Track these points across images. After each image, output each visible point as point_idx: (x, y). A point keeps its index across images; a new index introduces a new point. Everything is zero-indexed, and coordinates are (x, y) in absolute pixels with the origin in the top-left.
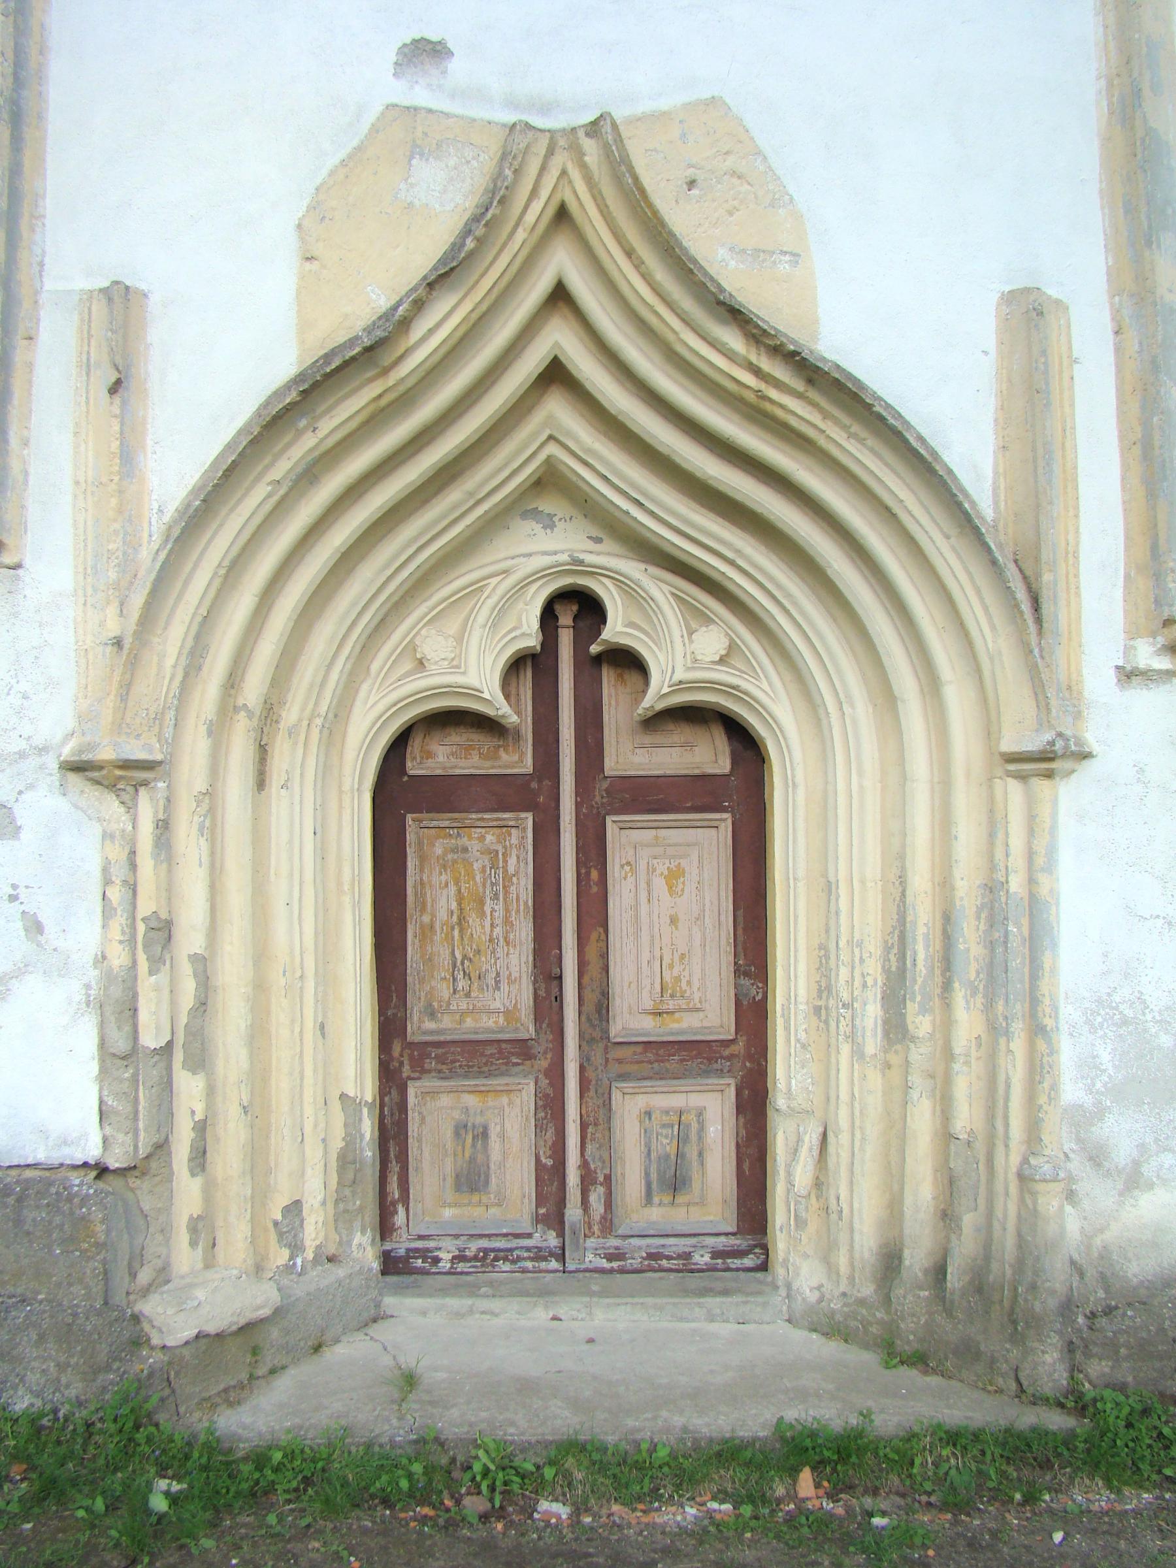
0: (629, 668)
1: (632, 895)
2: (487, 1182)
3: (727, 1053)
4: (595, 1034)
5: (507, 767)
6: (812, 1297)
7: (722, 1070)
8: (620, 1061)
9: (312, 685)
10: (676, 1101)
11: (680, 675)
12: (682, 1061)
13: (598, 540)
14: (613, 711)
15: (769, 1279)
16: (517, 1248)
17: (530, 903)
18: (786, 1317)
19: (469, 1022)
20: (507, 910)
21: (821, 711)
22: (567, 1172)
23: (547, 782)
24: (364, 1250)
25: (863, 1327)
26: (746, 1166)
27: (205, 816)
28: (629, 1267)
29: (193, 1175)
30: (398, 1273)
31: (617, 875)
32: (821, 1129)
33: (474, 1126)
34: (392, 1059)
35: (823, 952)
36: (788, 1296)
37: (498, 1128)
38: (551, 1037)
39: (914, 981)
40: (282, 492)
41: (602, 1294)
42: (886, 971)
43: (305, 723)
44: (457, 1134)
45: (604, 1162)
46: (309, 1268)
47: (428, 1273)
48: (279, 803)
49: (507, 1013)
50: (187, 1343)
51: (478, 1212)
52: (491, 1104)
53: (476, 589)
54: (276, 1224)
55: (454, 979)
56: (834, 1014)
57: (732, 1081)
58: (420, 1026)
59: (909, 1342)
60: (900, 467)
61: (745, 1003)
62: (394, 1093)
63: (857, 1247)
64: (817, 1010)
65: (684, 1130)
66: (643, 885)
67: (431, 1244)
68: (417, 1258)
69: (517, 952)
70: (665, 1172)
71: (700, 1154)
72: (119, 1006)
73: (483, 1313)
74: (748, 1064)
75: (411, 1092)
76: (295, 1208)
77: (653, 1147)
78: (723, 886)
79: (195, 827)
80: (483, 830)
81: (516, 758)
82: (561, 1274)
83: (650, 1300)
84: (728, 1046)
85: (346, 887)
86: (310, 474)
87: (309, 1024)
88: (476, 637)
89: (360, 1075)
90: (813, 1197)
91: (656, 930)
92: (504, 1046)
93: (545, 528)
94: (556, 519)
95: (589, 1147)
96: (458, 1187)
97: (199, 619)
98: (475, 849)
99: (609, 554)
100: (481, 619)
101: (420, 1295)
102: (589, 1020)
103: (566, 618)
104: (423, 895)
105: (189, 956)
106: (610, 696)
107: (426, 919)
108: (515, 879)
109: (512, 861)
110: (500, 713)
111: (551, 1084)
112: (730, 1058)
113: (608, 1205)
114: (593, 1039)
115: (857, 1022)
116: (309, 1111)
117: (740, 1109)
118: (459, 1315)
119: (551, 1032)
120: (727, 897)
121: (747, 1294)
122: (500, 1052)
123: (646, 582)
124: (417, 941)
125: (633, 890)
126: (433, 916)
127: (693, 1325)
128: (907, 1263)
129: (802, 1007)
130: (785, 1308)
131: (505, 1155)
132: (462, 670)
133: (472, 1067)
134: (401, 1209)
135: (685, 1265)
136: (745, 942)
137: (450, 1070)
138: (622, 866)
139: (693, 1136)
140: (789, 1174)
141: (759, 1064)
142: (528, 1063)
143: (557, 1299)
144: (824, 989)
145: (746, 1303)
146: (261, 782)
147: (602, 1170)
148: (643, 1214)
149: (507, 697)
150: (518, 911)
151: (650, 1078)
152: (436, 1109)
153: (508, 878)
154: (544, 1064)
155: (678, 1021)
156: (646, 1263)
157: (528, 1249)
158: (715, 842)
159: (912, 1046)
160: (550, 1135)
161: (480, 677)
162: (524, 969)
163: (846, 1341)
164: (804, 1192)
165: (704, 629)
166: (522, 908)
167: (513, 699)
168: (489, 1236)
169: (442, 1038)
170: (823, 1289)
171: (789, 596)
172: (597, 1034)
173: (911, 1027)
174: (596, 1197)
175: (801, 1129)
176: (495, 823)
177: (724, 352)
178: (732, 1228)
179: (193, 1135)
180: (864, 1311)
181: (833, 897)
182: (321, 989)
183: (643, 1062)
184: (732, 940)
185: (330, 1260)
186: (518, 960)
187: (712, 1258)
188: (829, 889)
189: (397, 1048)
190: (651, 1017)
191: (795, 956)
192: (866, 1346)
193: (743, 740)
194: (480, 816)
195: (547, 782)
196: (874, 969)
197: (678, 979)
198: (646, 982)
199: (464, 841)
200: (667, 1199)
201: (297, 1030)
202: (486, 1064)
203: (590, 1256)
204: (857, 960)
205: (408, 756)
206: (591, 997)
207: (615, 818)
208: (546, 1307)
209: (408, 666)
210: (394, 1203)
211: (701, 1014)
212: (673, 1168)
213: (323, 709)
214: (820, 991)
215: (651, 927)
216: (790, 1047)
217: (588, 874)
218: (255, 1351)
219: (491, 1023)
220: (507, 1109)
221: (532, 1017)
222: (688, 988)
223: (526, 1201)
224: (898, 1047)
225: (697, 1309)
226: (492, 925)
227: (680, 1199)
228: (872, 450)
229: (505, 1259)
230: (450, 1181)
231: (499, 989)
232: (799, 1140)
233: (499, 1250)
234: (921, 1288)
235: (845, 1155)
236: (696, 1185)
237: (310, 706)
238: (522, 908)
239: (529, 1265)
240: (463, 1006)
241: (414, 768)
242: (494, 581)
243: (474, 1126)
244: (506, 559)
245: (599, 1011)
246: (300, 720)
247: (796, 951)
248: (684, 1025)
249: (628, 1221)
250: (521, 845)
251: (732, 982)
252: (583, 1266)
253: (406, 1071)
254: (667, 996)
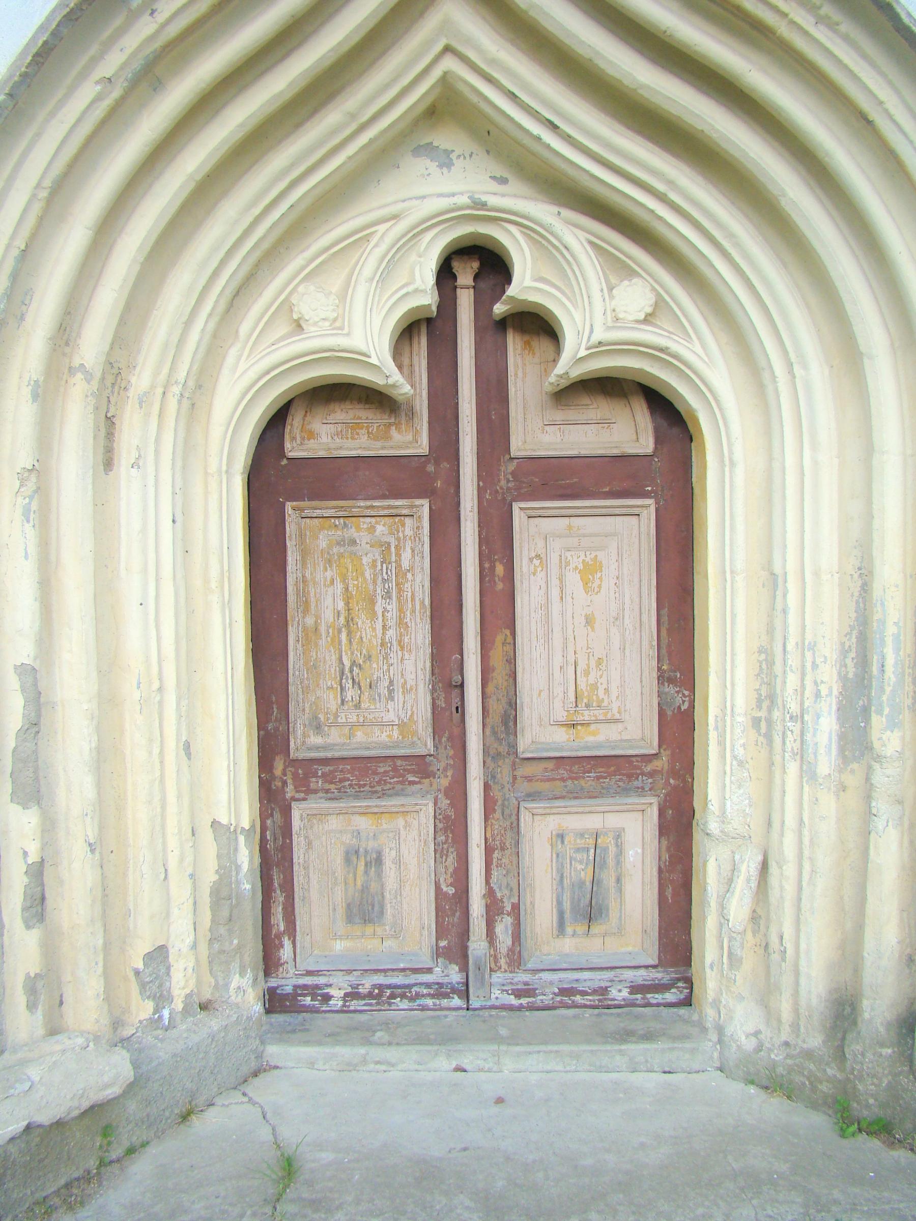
0: (538, 334)
1: (542, 592)
2: (382, 913)
3: (649, 768)
4: (501, 749)
5: (400, 447)
6: (749, 1044)
7: (643, 788)
8: (529, 779)
9: (166, 345)
10: (593, 822)
11: (600, 335)
12: (598, 778)
13: (503, 181)
14: (520, 383)
15: (695, 1017)
16: (416, 984)
17: (427, 602)
18: (717, 1064)
19: (360, 736)
20: (401, 610)
21: (766, 375)
22: (471, 901)
23: (445, 465)
24: (244, 992)
25: (811, 1083)
26: (669, 892)
27: (31, 498)
28: (539, 1003)
29: (28, 927)
30: (284, 1010)
31: (525, 569)
32: (760, 858)
33: (366, 851)
34: (274, 778)
35: (763, 656)
36: (720, 1041)
37: (393, 853)
38: (451, 753)
39: (882, 689)
40: (116, 93)
41: (513, 1040)
42: (843, 678)
43: (160, 390)
44: (347, 860)
45: (511, 890)
46: (178, 1018)
47: (317, 1011)
48: (130, 485)
49: (402, 726)
50: (12, 1139)
51: (372, 944)
52: (385, 826)
53: (359, 239)
54: (137, 973)
55: (342, 689)
56: (779, 727)
57: (654, 800)
58: (305, 741)
59: (869, 1105)
60: (882, 60)
61: (669, 713)
62: (277, 816)
63: (803, 992)
64: (756, 722)
65: (601, 852)
66: (555, 582)
67: (322, 980)
68: (305, 995)
69: (413, 658)
70: (579, 900)
71: (618, 880)
73: (377, 1063)
74: (672, 781)
75: (296, 814)
76: (159, 955)
77: (566, 873)
78: (645, 582)
79: (19, 511)
80: (373, 520)
81: (410, 437)
82: (464, 1012)
83: (566, 1048)
84: (650, 761)
85: (214, 585)
86: (151, 74)
87: (171, 744)
88: (361, 291)
89: (234, 800)
90: (749, 934)
91: (570, 632)
92: (399, 763)
93: (441, 166)
94: (453, 156)
95: (495, 873)
96: (350, 919)
97: (15, 252)
98: (364, 542)
99: (515, 196)
100: (368, 271)
101: (307, 1043)
102: (494, 733)
103: (465, 275)
104: (306, 594)
105: (16, 667)
106: (516, 366)
107: (310, 621)
108: (409, 576)
109: (406, 556)
110: (390, 381)
111: (452, 805)
112: (651, 774)
113: (517, 936)
114: (499, 754)
115: (808, 737)
116: (173, 843)
117: (663, 830)
118: (351, 1066)
119: (452, 747)
120: (649, 595)
121: (675, 1039)
122: (395, 769)
123: (559, 227)
124: (299, 646)
125: (544, 586)
126: (318, 617)
127: (614, 1076)
128: (866, 1015)
129: (740, 719)
130: (716, 1055)
131: (401, 882)
132: (346, 331)
133: (365, 785)
134: (287, 942)
135: (601, 999)
136: (669, 646)
137: (339, 790)
138: (531, 560)
139: (611, 862)
140: (722, 907)
141: (684, 781)
142: (427, 781)
143: (460, 1047)
144: (767, 697)
145: (673, 1049)
146: (108, 461)
147: (510, 897)
148: (555, 945)
149: (400, 367)
150: (413, 611)
151: (563, 797)
152: (324, 832)
153: (401, 573)
154: (445, 782)
155: (594, 734)
156: (558, 999)
157: (428, 985)
158: (635, 532)
159: (876, 766)
160: (451, 860)
162: (421, 676)
163: (789, 1097)
164: (740, 928)
165: (626, 283)
166: (418, 607)
167: (405, 369)
168: (385, 971)
169: (329, 755)
170: (762, 1036)
171: (731, 236)
172: (503, 749)
173: (876, 744)
174: (503, 928)
175: (737, 857)
176: (386, 512)
178: (656, 962)
179: (26, 880)
180: (812, 1066)
181: (779, 593)
182: (184, 703)
183: (554, 779)
184: (655, 643)
185: (204, 1007)
186: (414, 666)
187: (631, 993)
188: (773, 582)
189: (279, 766)
190: (564, 729)
191: (733, 661)
192: (814, 1106)
193: (669, 414)
194: (369, 503)
195: (445, 465)
196: (828, 676)
197: (595, 687)
198: (558, 691)
199: (352, 532)
200: (581, 929)
201: (156, 751)
202: (379, 783)
203: (496, 993)
204: (808, 665)
205: (287, 437)
206: (497, 708)
207: (523, 505)
208: (449, 1056)
209: (282, 328)
210: (279, 936)
211: (620, 726)
212: (589, 896)
213: (181, 375)
214: (759, 702)
215: (564, 629)
216: (725, 765)
217: (492, 568)
218: (107, 1131)
219: (384, 737)
220: (403, 832)
221: (430, 730)
222: (606, 698)
223: (426, 932)
224: (855, 766)
225: (618, 1057)
226: (384, 627)
227: (595, 929)
228: (846, 38)
229: (403, 996)
230: (341, 912)
231: (393, 700)
232: (734, 869)
233: (397, 987)
234: (882, 1045)
235: (790, 889)
236: (614, 914)
237: (165, 371)
238: (418, 607)
239: (429, 1002)
240: (353, 718)
241: (294, 448)
242: (382, 228)
243: (366, 851)
244: (396, 202)
245: (505, 722)
246: (153, 387)
247: (733, 655)
248: (601, 738)
249: (538, 953)
250: (417, 537)
251: (655, 689)
252: (489, 1003)
253: (290, 791)
254: (582, 706)
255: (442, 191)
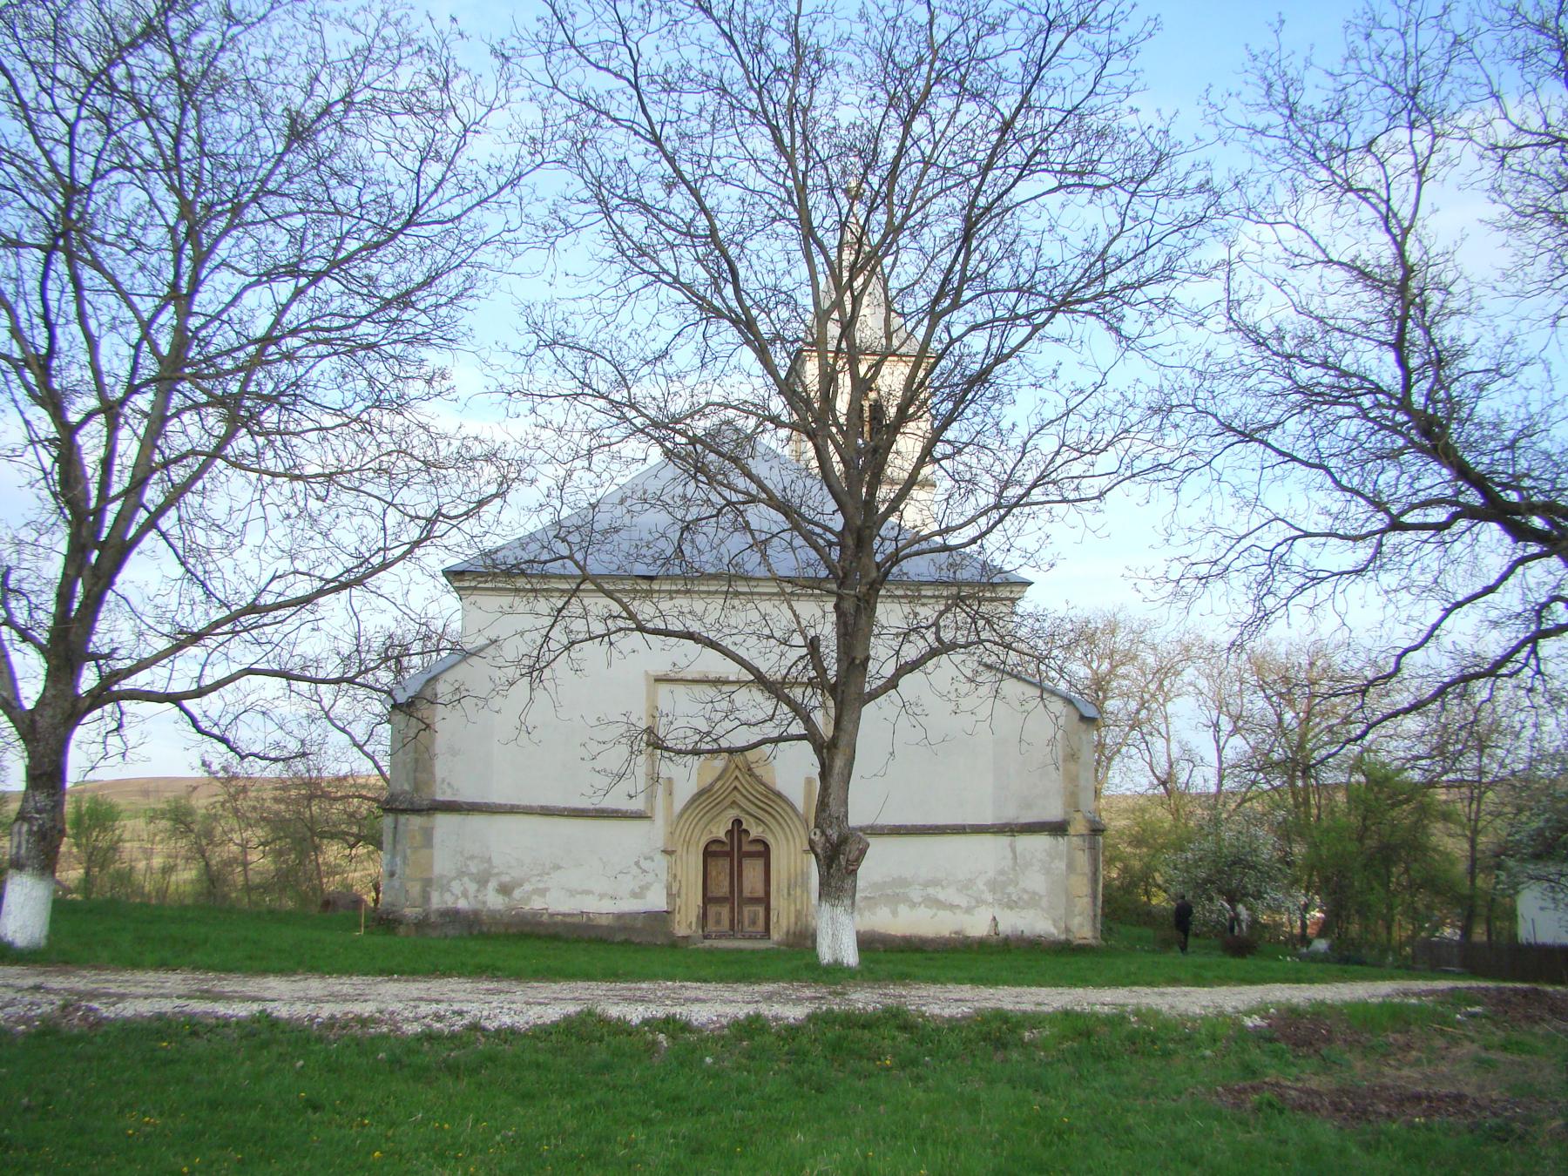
65: (756, 914)
72: (669, 888)
152: (713, 910)
161: (721, 834)
177: (761, 789)
186: (727, 883)
193: (767, 846)
255: (734, 813)
